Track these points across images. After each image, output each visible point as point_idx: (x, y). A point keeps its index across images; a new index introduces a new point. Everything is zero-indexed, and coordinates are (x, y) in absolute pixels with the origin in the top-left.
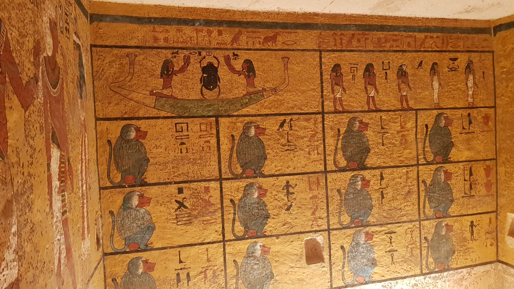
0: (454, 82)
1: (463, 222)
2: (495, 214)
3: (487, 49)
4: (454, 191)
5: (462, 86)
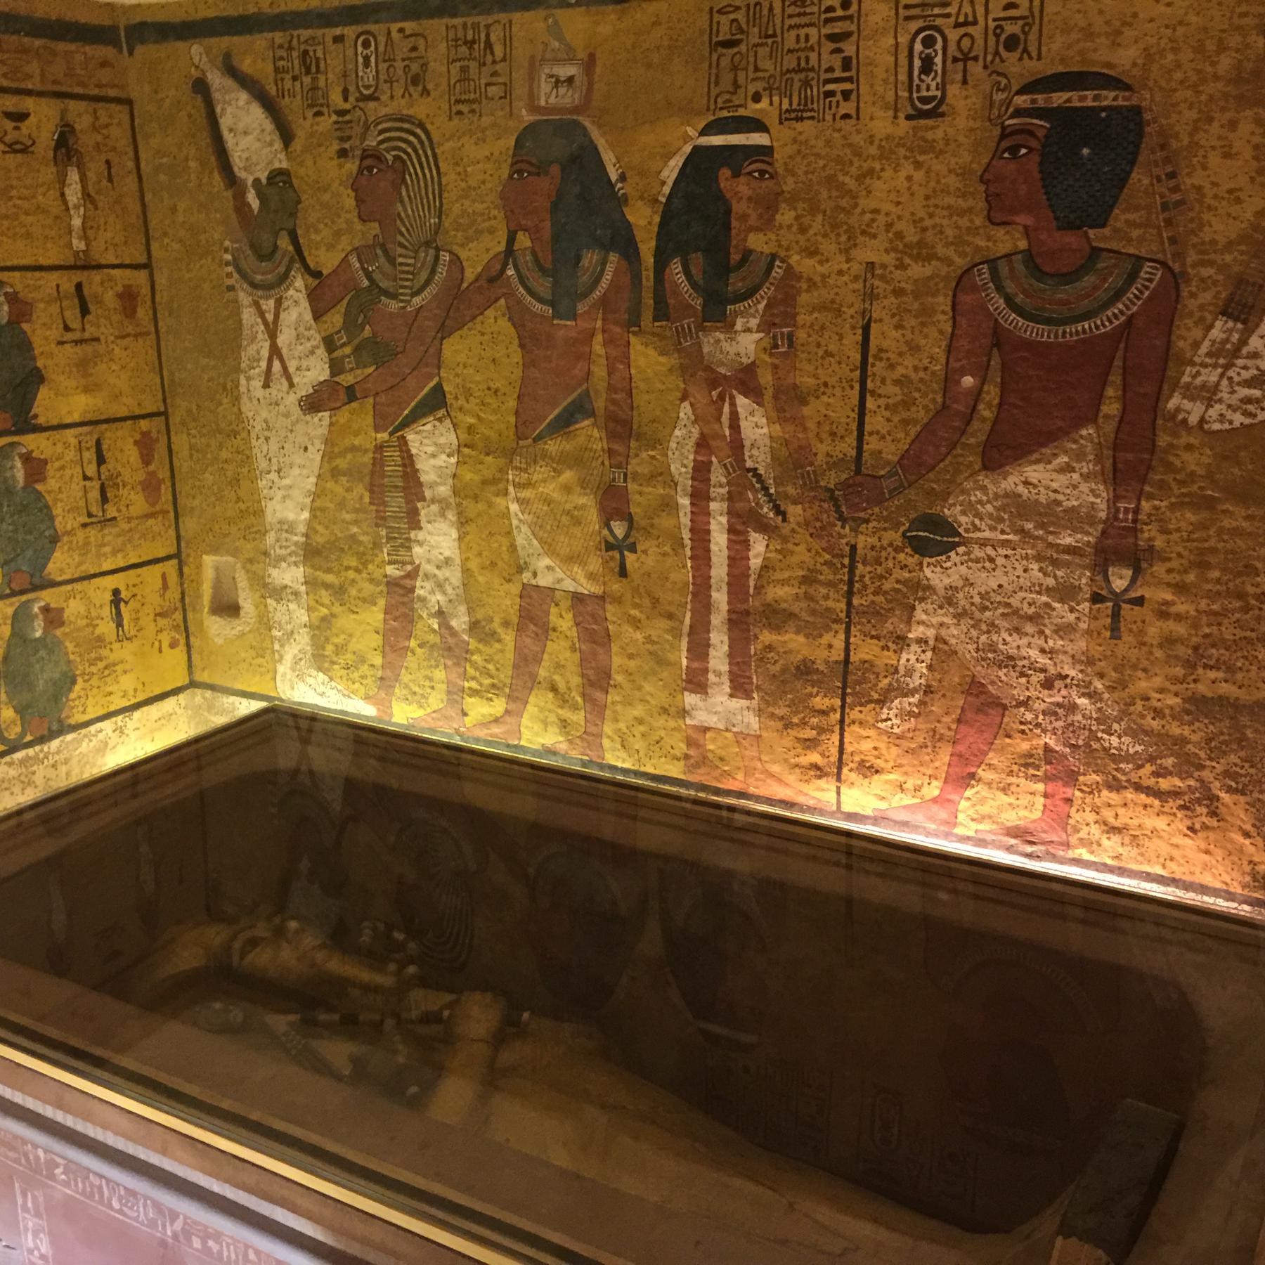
0: (26, 187)
1: (92, 594)
2: (174, 562)
3: (112, 93)
4: (57, 511)
5: (48, 199)
